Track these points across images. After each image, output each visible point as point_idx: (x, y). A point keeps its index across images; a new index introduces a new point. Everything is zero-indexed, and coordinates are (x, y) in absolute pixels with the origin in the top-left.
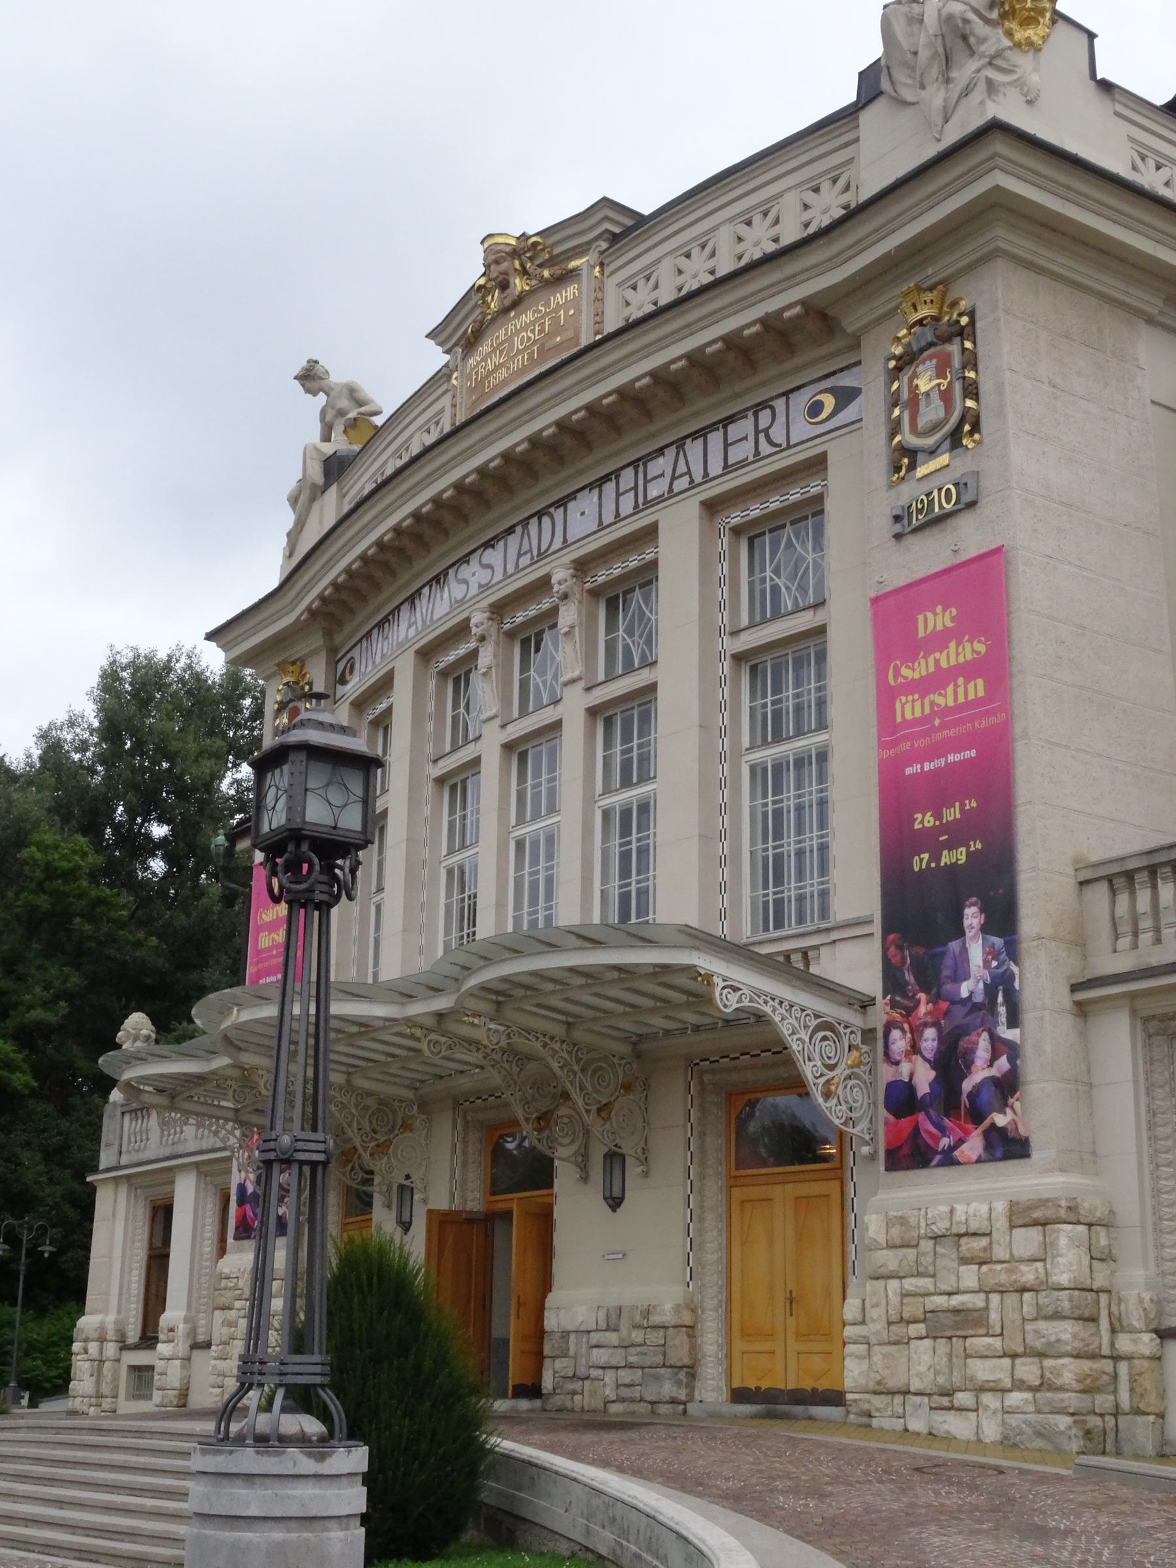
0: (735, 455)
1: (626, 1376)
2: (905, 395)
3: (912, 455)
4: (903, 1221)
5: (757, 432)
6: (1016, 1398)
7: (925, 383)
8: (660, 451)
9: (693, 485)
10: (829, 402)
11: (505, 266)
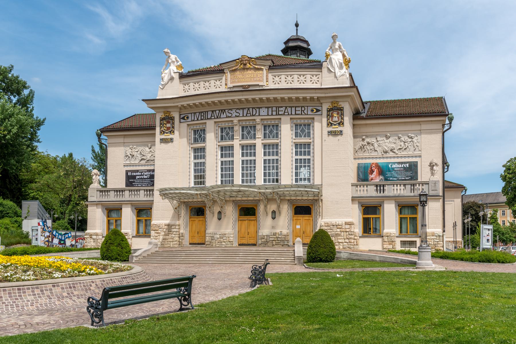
0: (297, 112)
3: (332, 124)
4: (327, 223)
6: (345, 244)
8: (282, 107)
9: (289, 114)
10: (315, 111)
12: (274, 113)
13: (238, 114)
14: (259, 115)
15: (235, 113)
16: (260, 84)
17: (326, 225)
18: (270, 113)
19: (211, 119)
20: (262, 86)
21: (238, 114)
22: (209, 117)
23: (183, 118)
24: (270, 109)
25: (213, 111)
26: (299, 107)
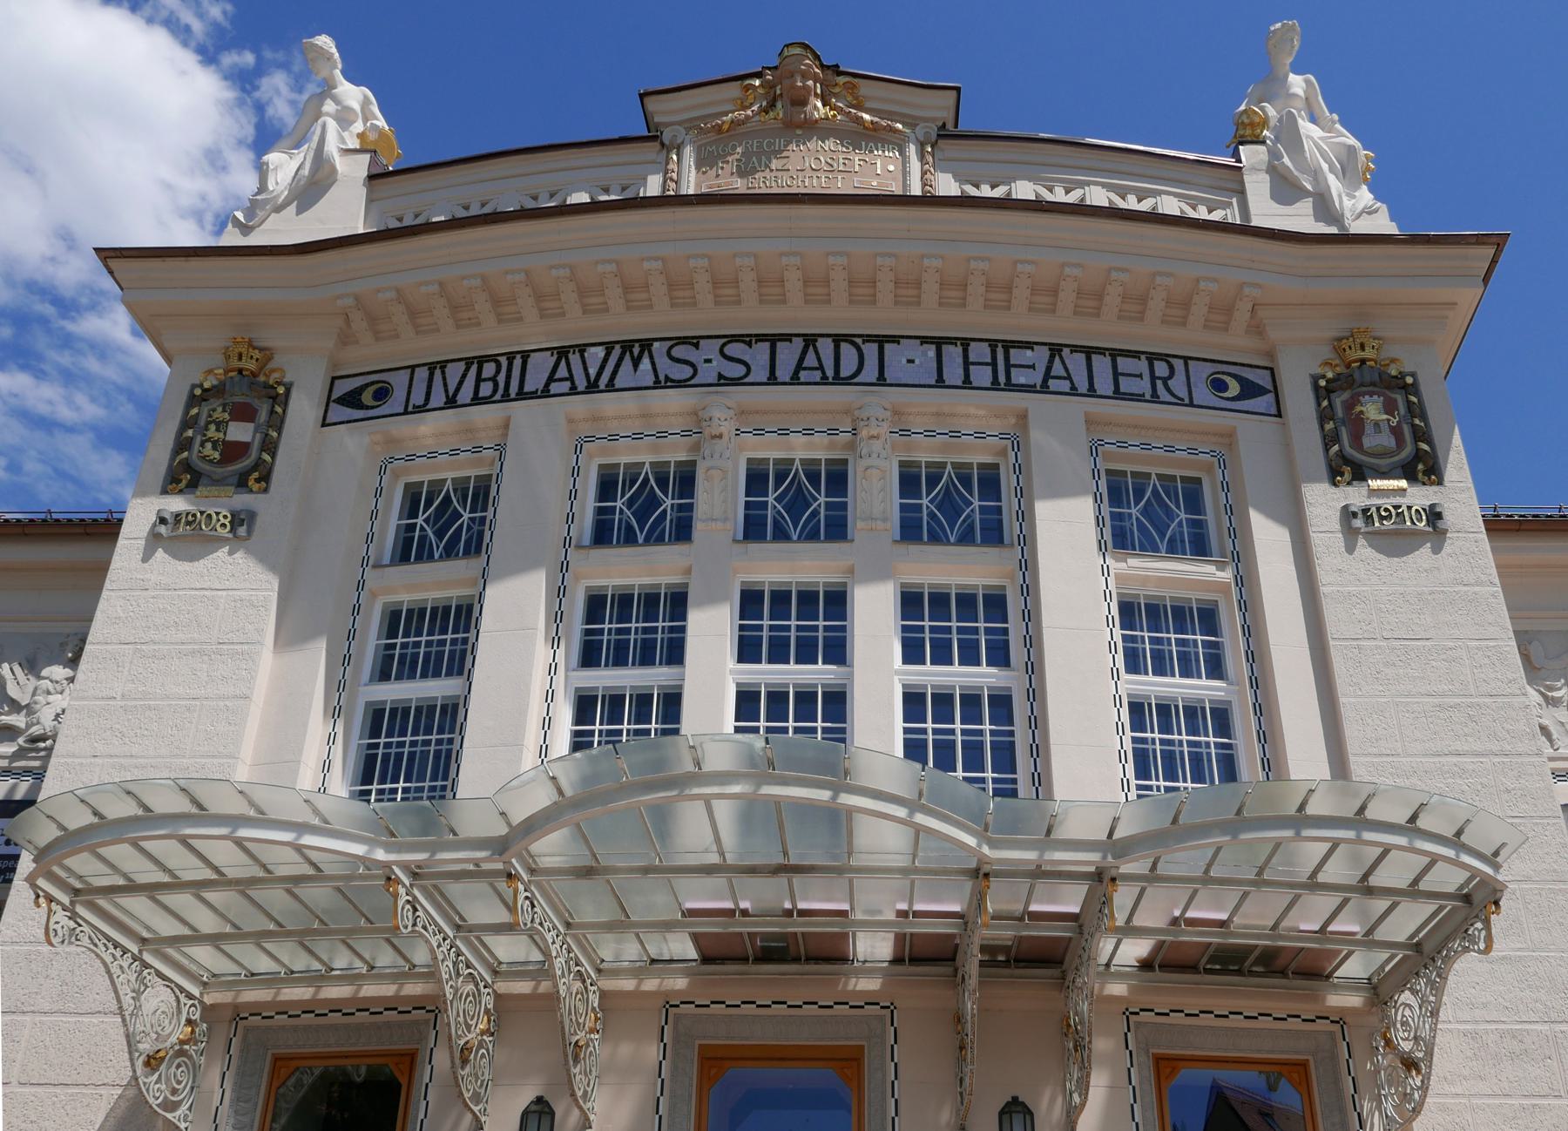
0: (1126, 385)
2: (1340, 413)
5: (1153, 378)
7: (1372, 409)
8: (1029, 345)
9: (1074, 392)
10: (1234, 388)
12: (982, 375)
13: (737, 371)
14: (881, 380)
15: (719, 364)
18: (954, 373)
19: (545, 393)
21: (739, 371)
22: (534, 382)
23: (352, 399)
24: (953, 354)
25: (562, 353)
26: (1135, 354)
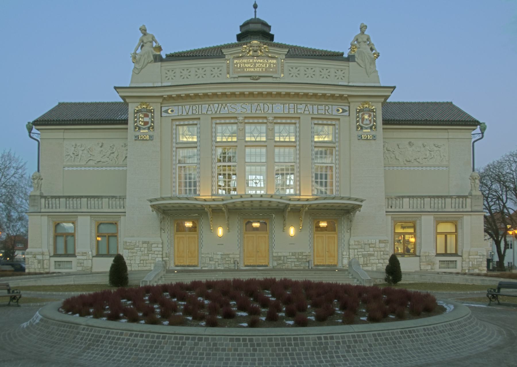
1: (296, 263)
4: (358, 241)
11: (257, 48)
16: (274, 76)
17: (357, 243)
20: (276, 78)
